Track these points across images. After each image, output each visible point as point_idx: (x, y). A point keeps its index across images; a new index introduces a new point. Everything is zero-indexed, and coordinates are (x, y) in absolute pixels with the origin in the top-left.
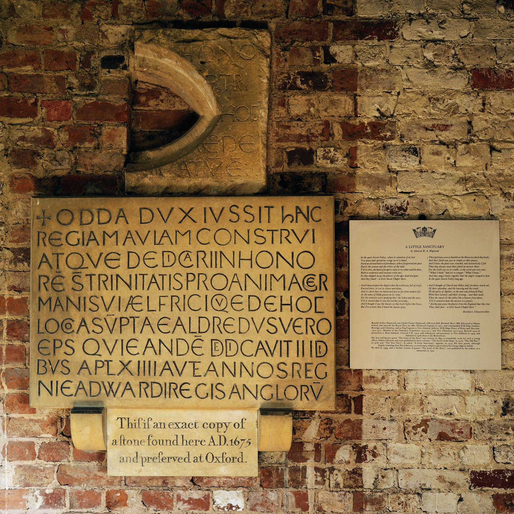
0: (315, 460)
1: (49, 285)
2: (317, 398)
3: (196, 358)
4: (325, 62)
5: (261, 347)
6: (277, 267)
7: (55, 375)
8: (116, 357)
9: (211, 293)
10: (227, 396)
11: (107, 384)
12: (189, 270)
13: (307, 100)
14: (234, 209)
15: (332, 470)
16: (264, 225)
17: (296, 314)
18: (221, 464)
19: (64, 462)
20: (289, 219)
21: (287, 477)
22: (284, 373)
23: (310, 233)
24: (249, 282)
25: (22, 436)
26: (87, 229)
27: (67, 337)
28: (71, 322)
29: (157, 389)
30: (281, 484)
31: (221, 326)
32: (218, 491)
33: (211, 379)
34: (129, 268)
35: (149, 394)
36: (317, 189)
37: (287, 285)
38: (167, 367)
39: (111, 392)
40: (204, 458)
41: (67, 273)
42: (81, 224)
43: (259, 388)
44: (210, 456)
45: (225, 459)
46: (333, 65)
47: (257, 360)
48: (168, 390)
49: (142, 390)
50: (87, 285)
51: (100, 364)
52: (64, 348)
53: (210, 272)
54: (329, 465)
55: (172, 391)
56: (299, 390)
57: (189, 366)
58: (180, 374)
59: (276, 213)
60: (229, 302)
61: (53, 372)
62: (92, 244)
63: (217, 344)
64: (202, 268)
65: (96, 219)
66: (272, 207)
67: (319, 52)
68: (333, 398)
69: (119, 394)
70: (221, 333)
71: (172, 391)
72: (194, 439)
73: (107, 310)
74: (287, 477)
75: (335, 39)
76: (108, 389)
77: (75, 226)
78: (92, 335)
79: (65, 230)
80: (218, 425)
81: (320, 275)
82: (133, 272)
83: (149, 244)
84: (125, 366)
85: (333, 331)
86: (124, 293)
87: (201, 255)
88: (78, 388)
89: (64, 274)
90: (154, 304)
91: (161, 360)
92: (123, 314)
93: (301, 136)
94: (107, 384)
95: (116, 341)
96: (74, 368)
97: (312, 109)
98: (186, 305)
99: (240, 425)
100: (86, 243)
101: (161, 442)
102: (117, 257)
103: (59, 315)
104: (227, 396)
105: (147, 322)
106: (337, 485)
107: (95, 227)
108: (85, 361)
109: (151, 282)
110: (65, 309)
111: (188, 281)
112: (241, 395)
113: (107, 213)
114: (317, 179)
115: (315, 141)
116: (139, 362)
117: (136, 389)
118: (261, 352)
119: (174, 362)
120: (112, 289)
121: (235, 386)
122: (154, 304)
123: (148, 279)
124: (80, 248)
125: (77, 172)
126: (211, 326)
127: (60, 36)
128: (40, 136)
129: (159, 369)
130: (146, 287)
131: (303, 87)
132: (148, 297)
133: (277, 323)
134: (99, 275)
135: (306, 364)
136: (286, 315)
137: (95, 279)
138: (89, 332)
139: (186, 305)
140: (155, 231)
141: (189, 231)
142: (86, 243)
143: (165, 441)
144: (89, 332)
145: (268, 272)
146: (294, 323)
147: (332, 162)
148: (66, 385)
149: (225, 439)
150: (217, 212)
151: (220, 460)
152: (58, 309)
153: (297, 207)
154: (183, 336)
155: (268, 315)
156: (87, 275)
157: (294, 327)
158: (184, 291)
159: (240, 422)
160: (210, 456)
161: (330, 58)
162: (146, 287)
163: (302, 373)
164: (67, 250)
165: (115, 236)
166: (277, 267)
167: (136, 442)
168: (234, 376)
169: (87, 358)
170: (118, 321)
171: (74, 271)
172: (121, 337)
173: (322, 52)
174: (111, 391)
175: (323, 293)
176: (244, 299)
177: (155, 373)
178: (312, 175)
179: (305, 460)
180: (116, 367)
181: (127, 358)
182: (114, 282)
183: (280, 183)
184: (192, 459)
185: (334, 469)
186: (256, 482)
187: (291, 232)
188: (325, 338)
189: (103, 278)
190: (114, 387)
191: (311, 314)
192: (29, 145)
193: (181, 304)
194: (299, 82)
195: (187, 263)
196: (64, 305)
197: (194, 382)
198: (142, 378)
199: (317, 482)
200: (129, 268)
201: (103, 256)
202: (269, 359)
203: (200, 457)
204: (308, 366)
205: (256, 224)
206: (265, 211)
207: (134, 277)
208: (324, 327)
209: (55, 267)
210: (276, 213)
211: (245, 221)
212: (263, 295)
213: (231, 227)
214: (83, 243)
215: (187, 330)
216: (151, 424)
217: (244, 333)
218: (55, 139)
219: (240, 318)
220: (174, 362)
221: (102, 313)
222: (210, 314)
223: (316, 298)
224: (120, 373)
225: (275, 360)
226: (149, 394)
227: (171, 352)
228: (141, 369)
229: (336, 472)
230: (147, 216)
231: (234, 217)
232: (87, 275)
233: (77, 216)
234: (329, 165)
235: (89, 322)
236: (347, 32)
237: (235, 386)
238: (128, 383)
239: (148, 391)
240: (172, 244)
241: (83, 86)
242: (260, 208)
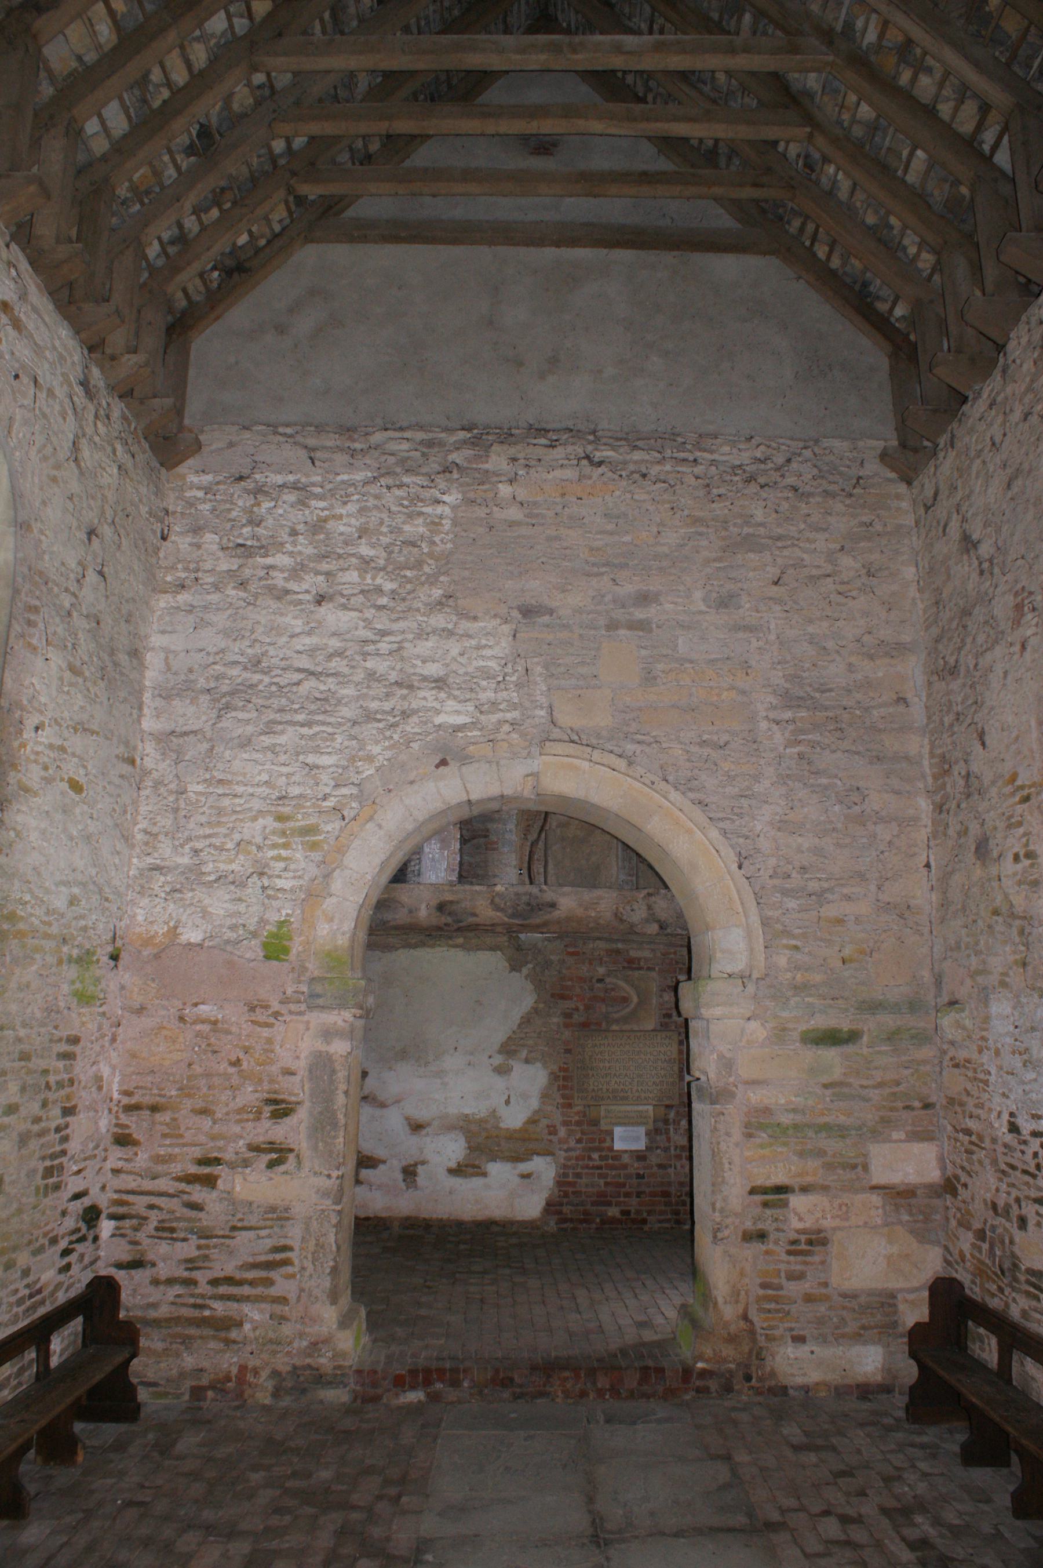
8: (605, 1087)
30: (661, 1134)
33: (637, 1094)
80: (638, 1111)
86: (607, 1065)
99: (647, 1111)
136: (663, 1072)
174: (602, 1099)
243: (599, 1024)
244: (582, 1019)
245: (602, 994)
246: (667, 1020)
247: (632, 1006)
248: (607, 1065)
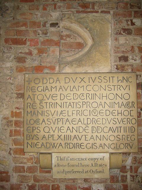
0: (130, 172)
1: (31, 106)
2: (131, 148)
3: (86, 134)
4: (131, 25)
5: (110, 129)
6: (116, 99)
7: (33, 140)
8: (56, 133)
9: (92, 109)
10: (98, 148)
11: (52, 144)
12: (83, 101)
13: (125, 38)
14: (100, 78)
15: (137, 176)
16: (111, 84)
17: (123, 117)
18: (95, 174)
19: (36, 174)
20: (120, 81)
21: (120, 179)
22: (119, 139)
23: (128, 86)
24: (106, 105)
25: (20, 163)
26: (45, 86)
27: (37, 126)
28: (39, 120)
29: (71, 146)
30: (117, 181)
31: (96, 121)
32: (94, 185)
33: (92, 141)
34: (61, 100)
35: (69, 148)
36: (130, 71)
37: (120, 106)
38: (75, 137)
39: (54, 147)
40: (89, 172)
41: (38, 102)
42: (43, 83)
43: (110, 145)
44: (91, 171)
45: (97, 172)
46: (134, 26)
47: (109, 134)
48: (75, 146)
49: (66, 146)
50: (45, 107)
51: (50, 136)
52: (37, 130)
53: (91, 101)
54: (136, 174)
55: (77, 146)
56: (125, 145)
57: (84, 137)
58: (80, 140)
59: (115, 79)
60: (98, 112)
61: (33, 139)
62: (47, 91)
63: (94, 129)
64: (88, 100)
65: (48, 82)
66: (114, 77)
67: (129, 22)
68: (137, 148)
69: (57, 147)
70: (96, 124)
71: (77, 146)
72: (85, 164)
73: (53, 116)
74: (120, 179)
75: (135, 17)
76: (53, 145)
77: (40, 84)
78: (47, 125)
79: (37, 86)
80: (95, 159)
81: (132, 102)
82: (62, 102)
83: (68, 91)
84: (60, 137)
85: (137, 123)
86: (59, 109)
87: (88, 95)
88: (42, 145)
89: (36, 102)
90: (70, 114)
91: (73, 135)
92: (58, 117)
93: (123, 51)
94: (52, 144)
95: (56, 127)
96: (40, 138)
97: (127, 42)
98: (83, 113)
99: (102, 159)
100: (44, 91)
101: (73, 166)
102: (56, 96)
103: (34, 118)
104: (98, 148)
105: (68, 120)
106: (139, 182)
107: (48, 84)
108: (44, 135)
109: (69, 105)
110: (37, 115)
111: (83, 105)
112: (103, 147)
113: (52, 79)
114: (130, 67)
115: (128, 53)
116: (65, 135)
117: (64, 146)
118: (110, 131)
119: (78, 135)
120: (54, 108)
121: (101, 144)
122: (70, 114)
123: (68, 104)
124: (42, 93)
125: (41, 64)
126: (92, 121)
127: (35, 16)
128: (27, 52)
129: (72, 138)
130: (67, 107)
131: (123, 33)
132: (68, 111)
133: (116, 120)
134: (50, 103)
135: (127, 135)
136: (120, 117)
137: (48, 104)
138: (46, 124)
139: (83, 113)
140: (70, 86)
141: (83, 86)
142: (44, 91)
143: (74, 165)
144: (46, 124)
145: (113, 101)
146: (123, 120)
147: (135, 61)
148: (37, 144)
149: (97, 164)
150: (94, 79)
151: (95, 172)
152: (34, 115)
153: (123, 77)
154: (81, 125)
155: (113, 117)
156: (45, 103)
157: (122, 121)
158: (81, 108)
159: (102, 158)
160: (91, 171)
161: (133, 24)
162: (67, 107)
163: (126, 139)
164: (37, 93)
165: (55, 88)
166: (116, 99)
167: (63, 166)
168: (101, 140)
169: (45, 134)
170: (57, 120)
171: (40, 101)
172: (58, 126)
173: (130, 21)
174: (54, 146)
175: (133, 109)
176: (104, 111)
177: (71, 140)
178: (128, 65)
179: (127, 172)
180: (56, 137)
181: (60, 134)
182: (55, 105)
183: (116, 69)
184: (84, 172)
185: (138, 176)
186: (108, 181)
187: (121, 86)
188: (134, 126)
189: (51, 104)
190: (55, 145)
191: (129, 116)
192: (23, 55)
193: (80, 113)
194: (122, 32)
195: (83, 98)
196: (37, 114)
197: (86, 142)
198: (66, 141)
199: (131, 181)
200: (61, 100)
201: (51, 95)
202: (114, 134)
203: (88, 171)
204: (128, 136)
205: (108, 83)
206: (111, 79)
207: (62, 103)
208: (134, 121)
209: (33, 100)
210: (115, 79)
211: (104, 82)
212: (111, 110)
213: (99, 84)
214: (44, 91)
215: (83, 123)
216: (69, 158)
217: (104, 124)
218: (33, 53)
219: (102, 119)
220: (78, 135)
221: (51, 117)
222: (91, 117)
223: (130, 111)
224: (57, 140)
225: (116, 134)
226: (69, 148)
227: (77, 132)
228: (66, 138)
229: (138, 177)
230: (67, 80)
231: (100, 81)
232: (45, 103)
233: (41, 80)
234: (134, 62)
235: (46, 120)
236: (139, 15)
237: (101, 144)
238: (60, 143)
239: (68, 146)
240: (77, 91)
241: (43, 33)
242: (110, 77)
243: (52, 68)
244: (36, 64)
245: (56, 38)
246: (123, 63)
247: (86, 49)
248: (59, 109)
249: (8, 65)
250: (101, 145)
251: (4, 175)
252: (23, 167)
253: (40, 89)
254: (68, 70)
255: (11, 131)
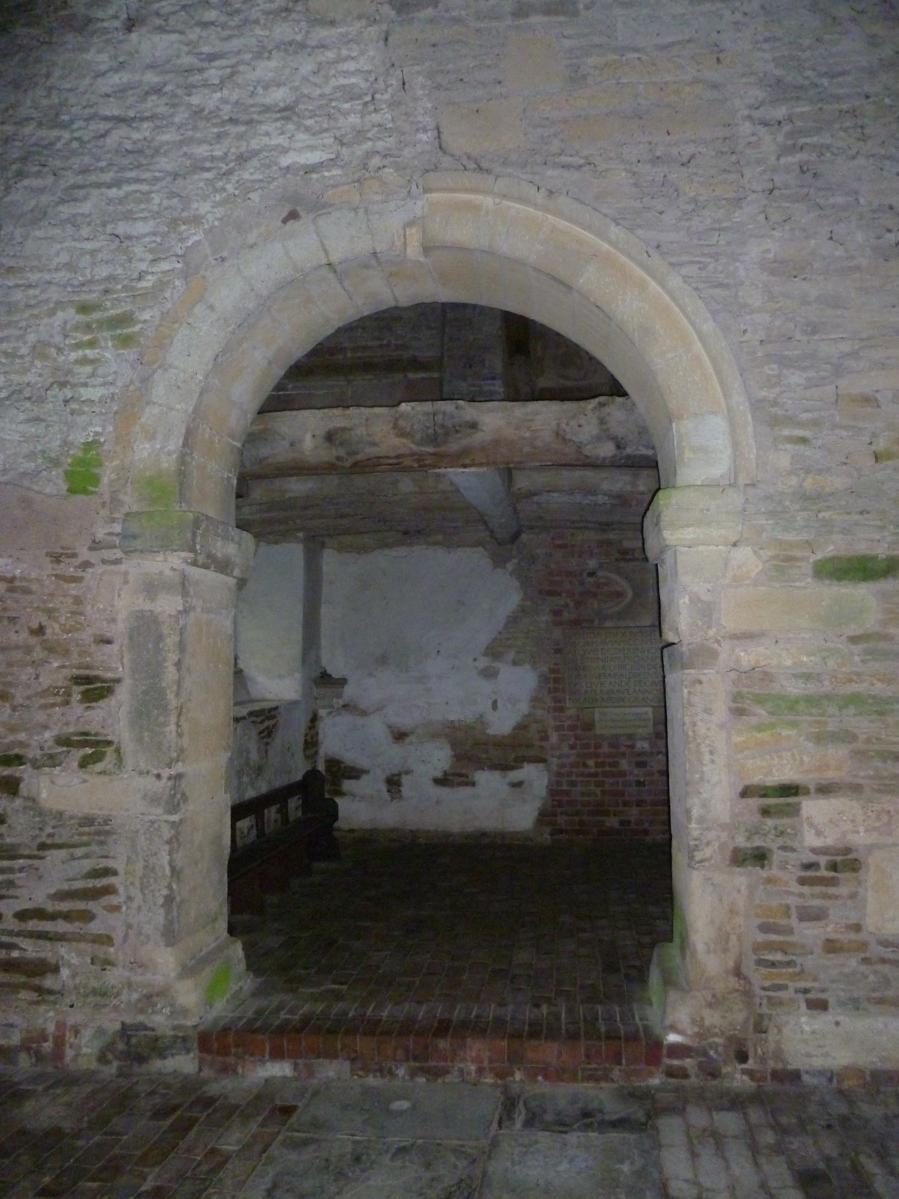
249: (544, 618)
250: (643, 699)
251: (543, 734)
252: (563, 726)
253: (581, 644)
254: (608, 624)
255: (549, 688)
